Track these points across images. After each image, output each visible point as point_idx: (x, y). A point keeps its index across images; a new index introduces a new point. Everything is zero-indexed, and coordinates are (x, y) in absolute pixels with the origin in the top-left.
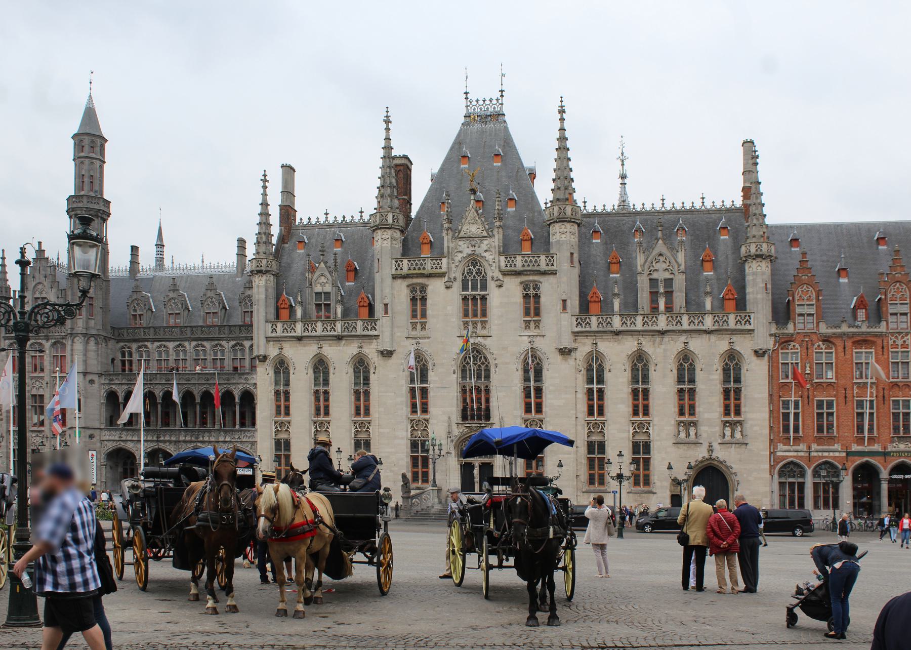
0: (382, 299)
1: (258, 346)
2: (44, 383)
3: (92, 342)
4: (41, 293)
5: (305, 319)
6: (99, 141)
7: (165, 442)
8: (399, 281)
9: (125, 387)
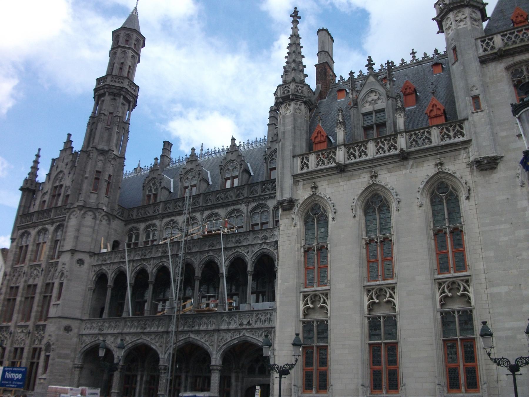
0: (468, 89)
1: (282, 188)
2: (40, 270)
3: (89, 217)
4: (60, 181)
5: (350, 145)
6: (135, 36)
7: (149, 334)
8: (492, 66)
9: (116, 267)
